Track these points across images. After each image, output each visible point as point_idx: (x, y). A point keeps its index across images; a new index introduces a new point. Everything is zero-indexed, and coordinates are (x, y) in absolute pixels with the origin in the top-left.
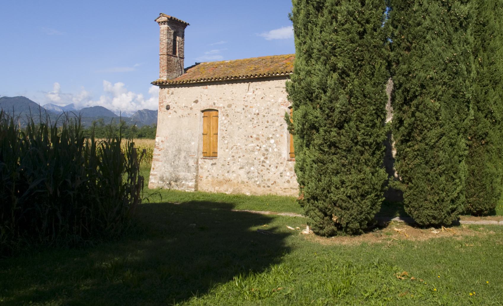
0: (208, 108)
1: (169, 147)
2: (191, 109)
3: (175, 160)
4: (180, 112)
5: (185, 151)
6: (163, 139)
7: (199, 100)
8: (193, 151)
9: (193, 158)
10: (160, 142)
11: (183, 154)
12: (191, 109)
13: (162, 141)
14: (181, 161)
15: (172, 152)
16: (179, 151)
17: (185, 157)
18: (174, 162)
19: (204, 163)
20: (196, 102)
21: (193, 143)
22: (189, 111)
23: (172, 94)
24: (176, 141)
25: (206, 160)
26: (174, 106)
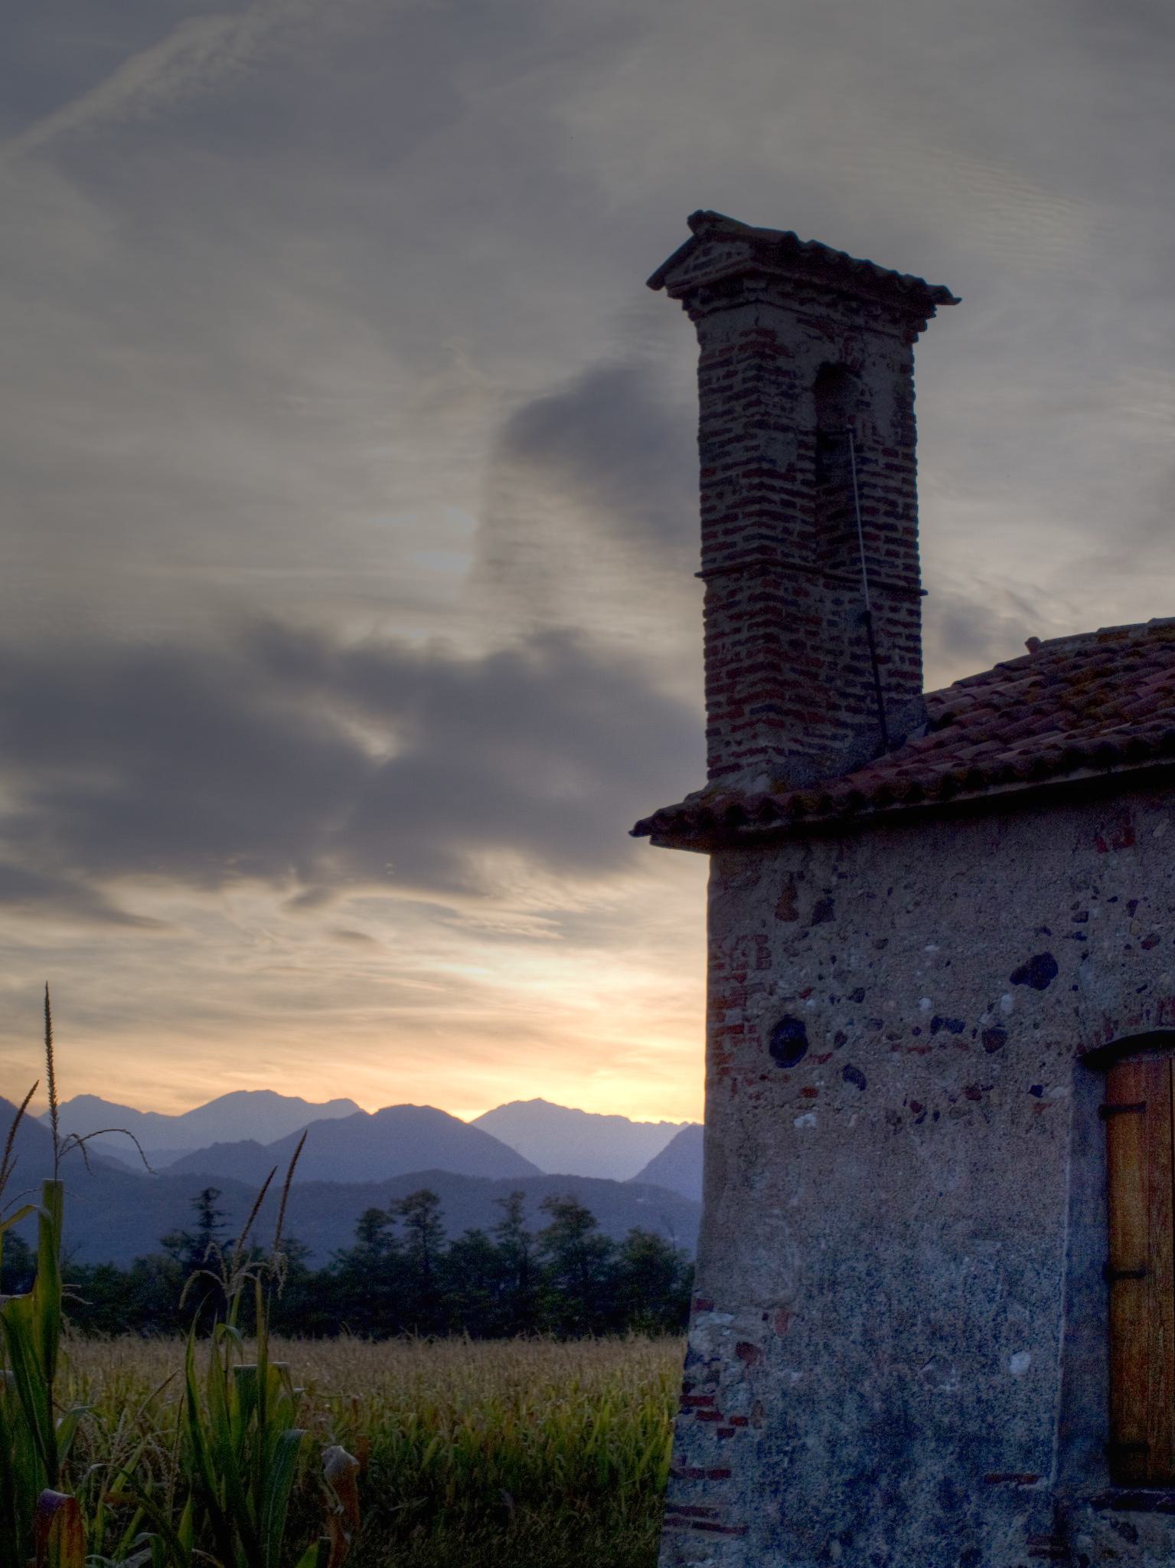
0: (1147, 1026)
1: (805, 1400)
2: (994, 1040)
3: (861, 1522)
4: (897, 1079)
5: (944, 1436)
6: (756, 1329)
7: (1066, 957)
8: (1018, 1431)
9: (1018, 1500)
10: (727, 1353)
11: (931, 1466)
12: (994, 1040)
13: (744, 1350)
14: (914, 1532)
15: (833, 1445)
16: (895, 1432)
17: (948, 1495)
18: (847, 1540)
19: (1119, 1544)
20: (1037, 973)
21: (1019, 1363)
22: (973, 1065)
23: (823, 912)
24: (870, 1342)
25: (1141, 1520)
26: (839, 1023)
